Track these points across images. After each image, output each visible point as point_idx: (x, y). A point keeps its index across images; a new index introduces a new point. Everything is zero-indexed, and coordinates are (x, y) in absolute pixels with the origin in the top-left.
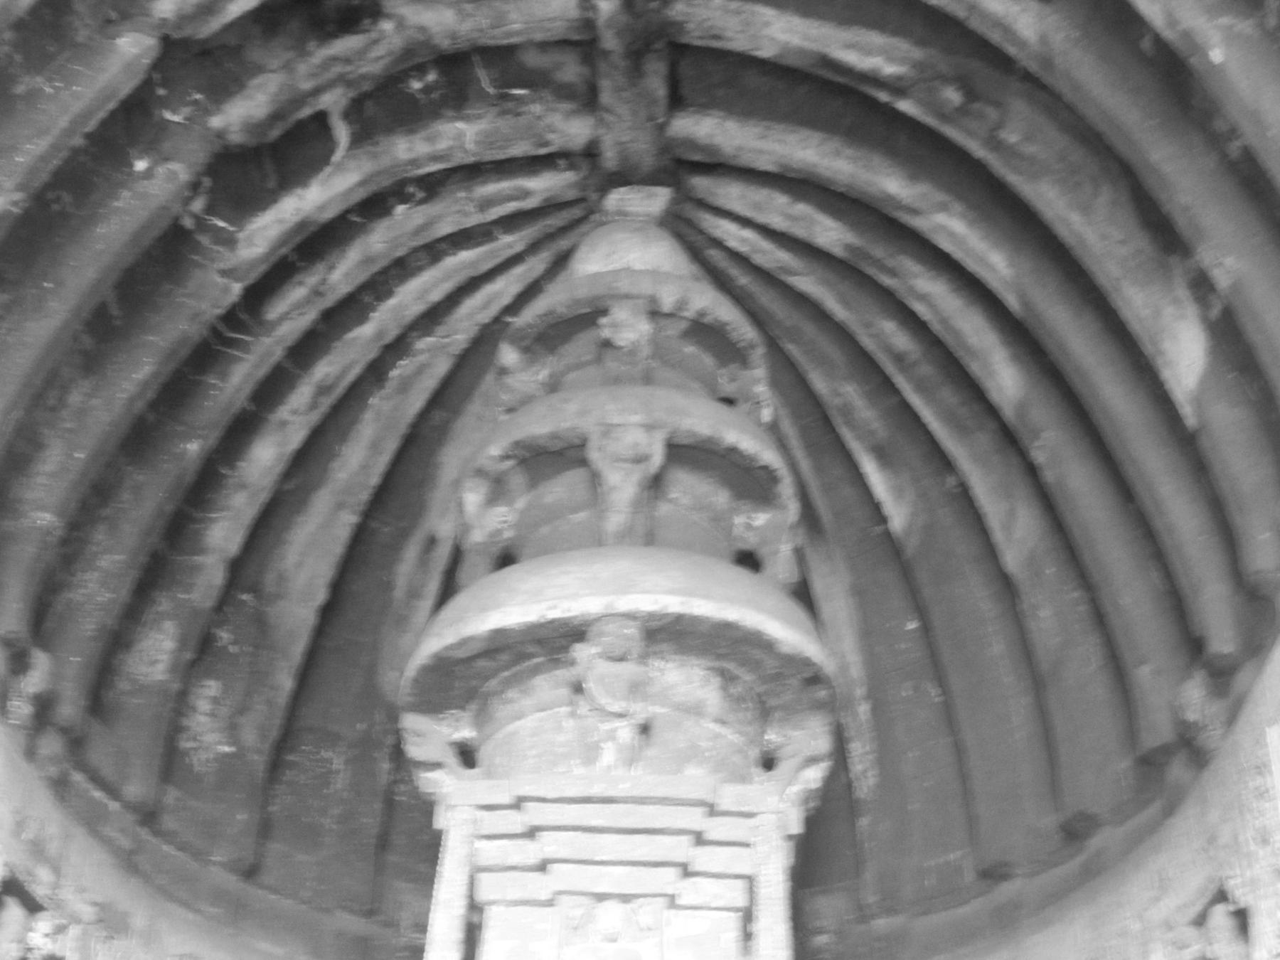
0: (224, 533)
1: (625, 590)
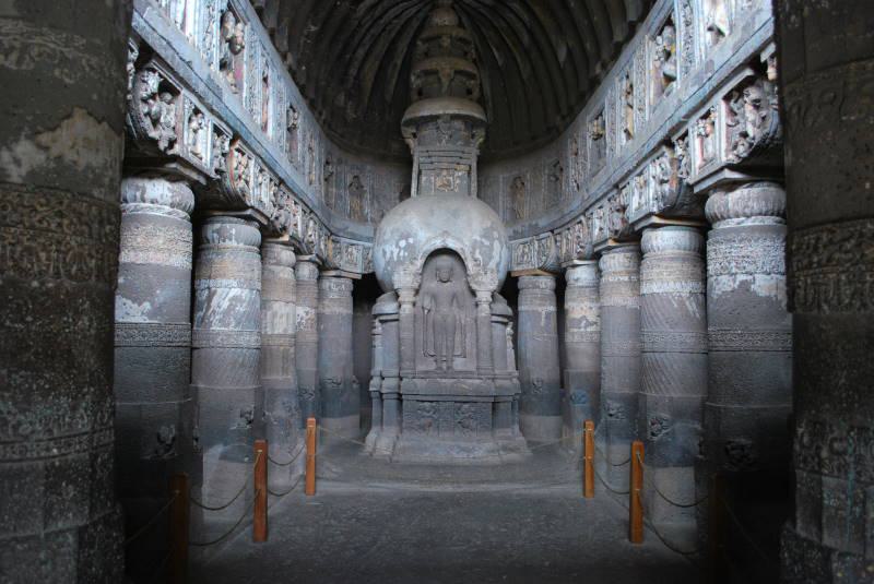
0: (353, 71)
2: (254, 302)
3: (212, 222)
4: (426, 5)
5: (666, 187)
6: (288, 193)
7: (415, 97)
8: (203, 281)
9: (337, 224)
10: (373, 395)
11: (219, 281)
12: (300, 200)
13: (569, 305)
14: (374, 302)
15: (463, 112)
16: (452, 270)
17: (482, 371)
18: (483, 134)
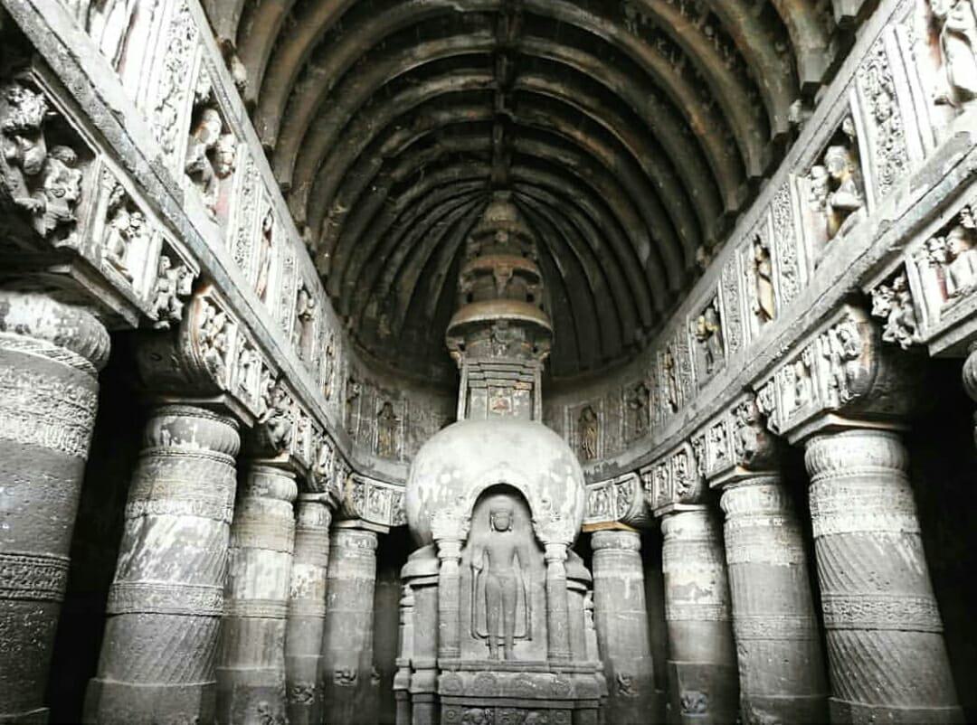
0: (389, 278)
1: (505, 313)
2: (218, 540)
3: (164, 414)
4: (476, 205)
5: (854, 367)
6: (291, 396)
7: (463, 300)
8: (138, 504)
9: (362, 459)
10: (398, 697)
11: (162, 502)
12: (308, 410)
14: (406, 561)
15: (523, 317)
16: (511, 514)
17: (555, 661)
18: (548, 347)
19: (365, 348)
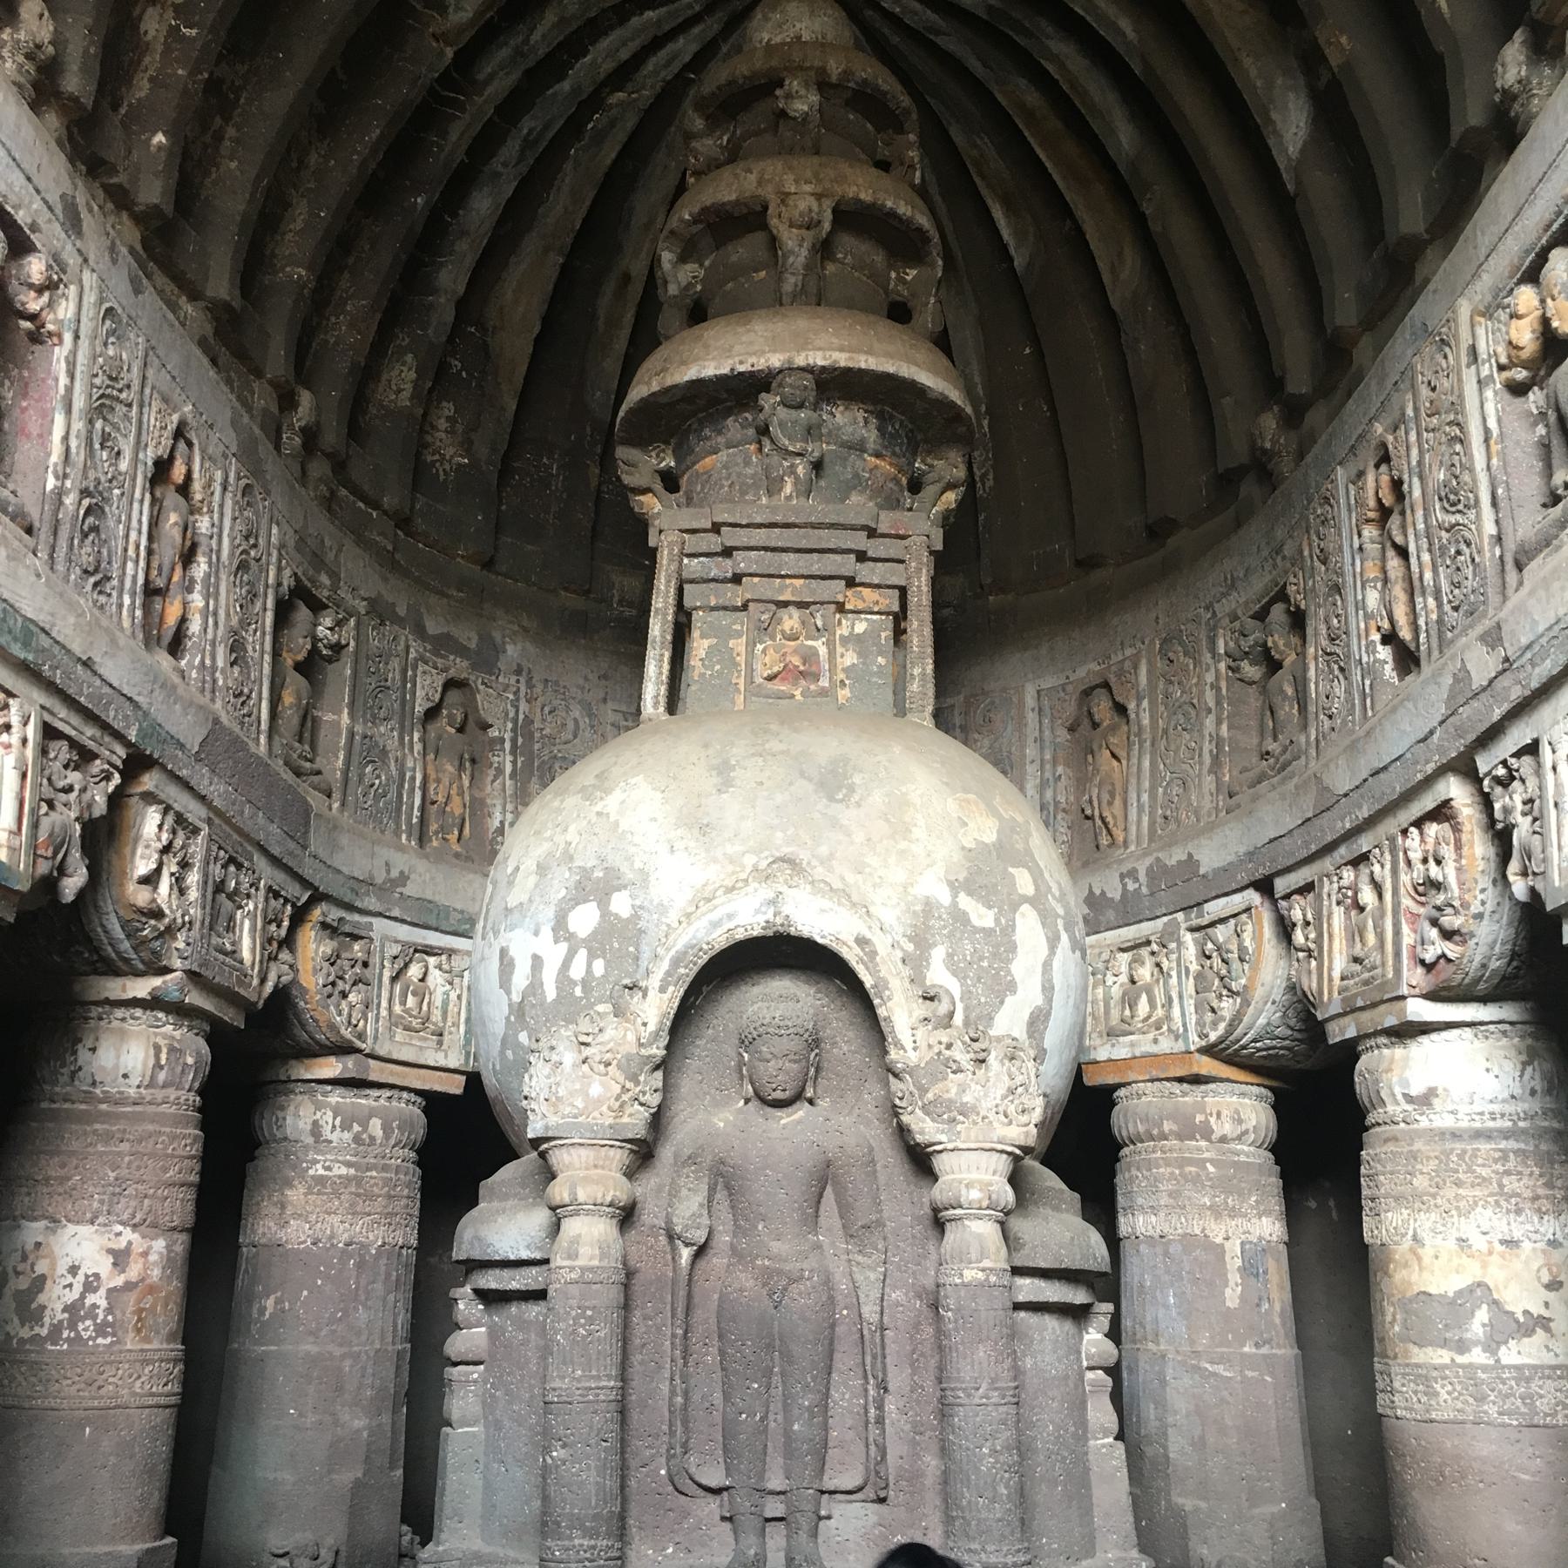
0: (451, 278)
1: (804, 347)
13: (1389, 1224)
18: (960, 473)
19: (376, 505)
